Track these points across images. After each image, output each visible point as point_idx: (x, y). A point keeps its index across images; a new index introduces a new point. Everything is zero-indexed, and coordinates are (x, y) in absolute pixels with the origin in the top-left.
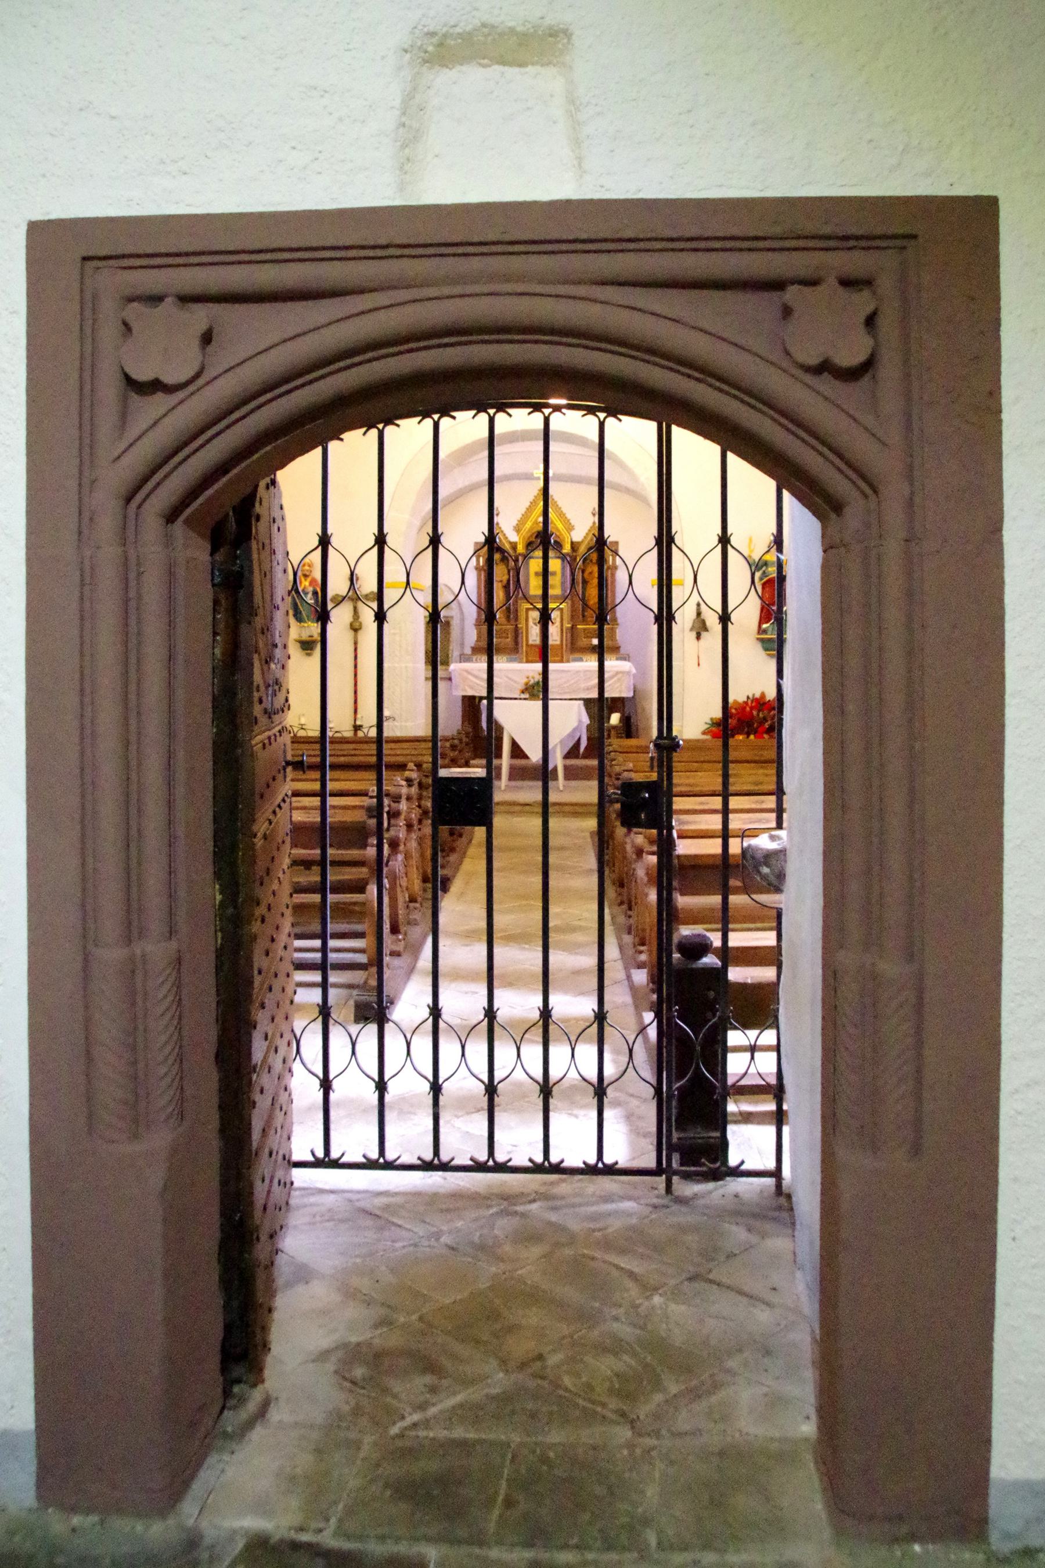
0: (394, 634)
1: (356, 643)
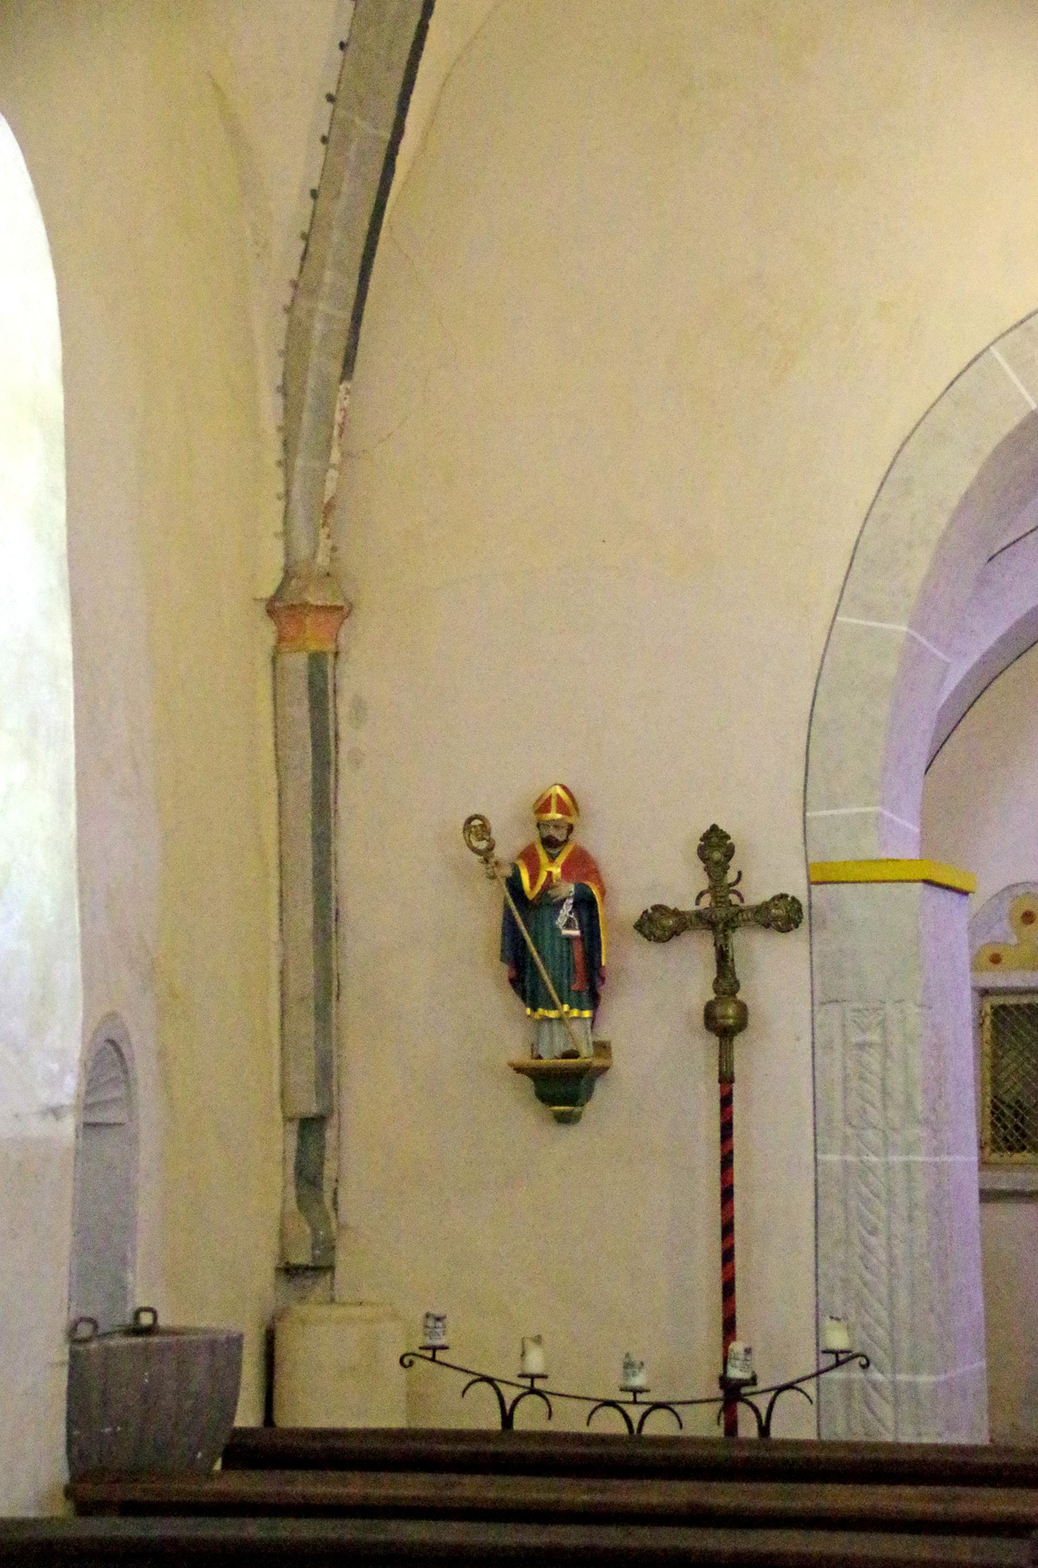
0: (862, 1046)
1: (726, 1080)
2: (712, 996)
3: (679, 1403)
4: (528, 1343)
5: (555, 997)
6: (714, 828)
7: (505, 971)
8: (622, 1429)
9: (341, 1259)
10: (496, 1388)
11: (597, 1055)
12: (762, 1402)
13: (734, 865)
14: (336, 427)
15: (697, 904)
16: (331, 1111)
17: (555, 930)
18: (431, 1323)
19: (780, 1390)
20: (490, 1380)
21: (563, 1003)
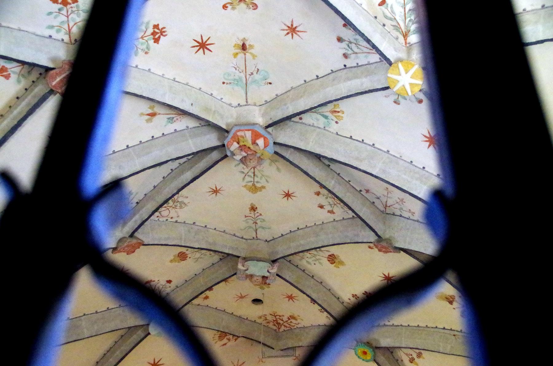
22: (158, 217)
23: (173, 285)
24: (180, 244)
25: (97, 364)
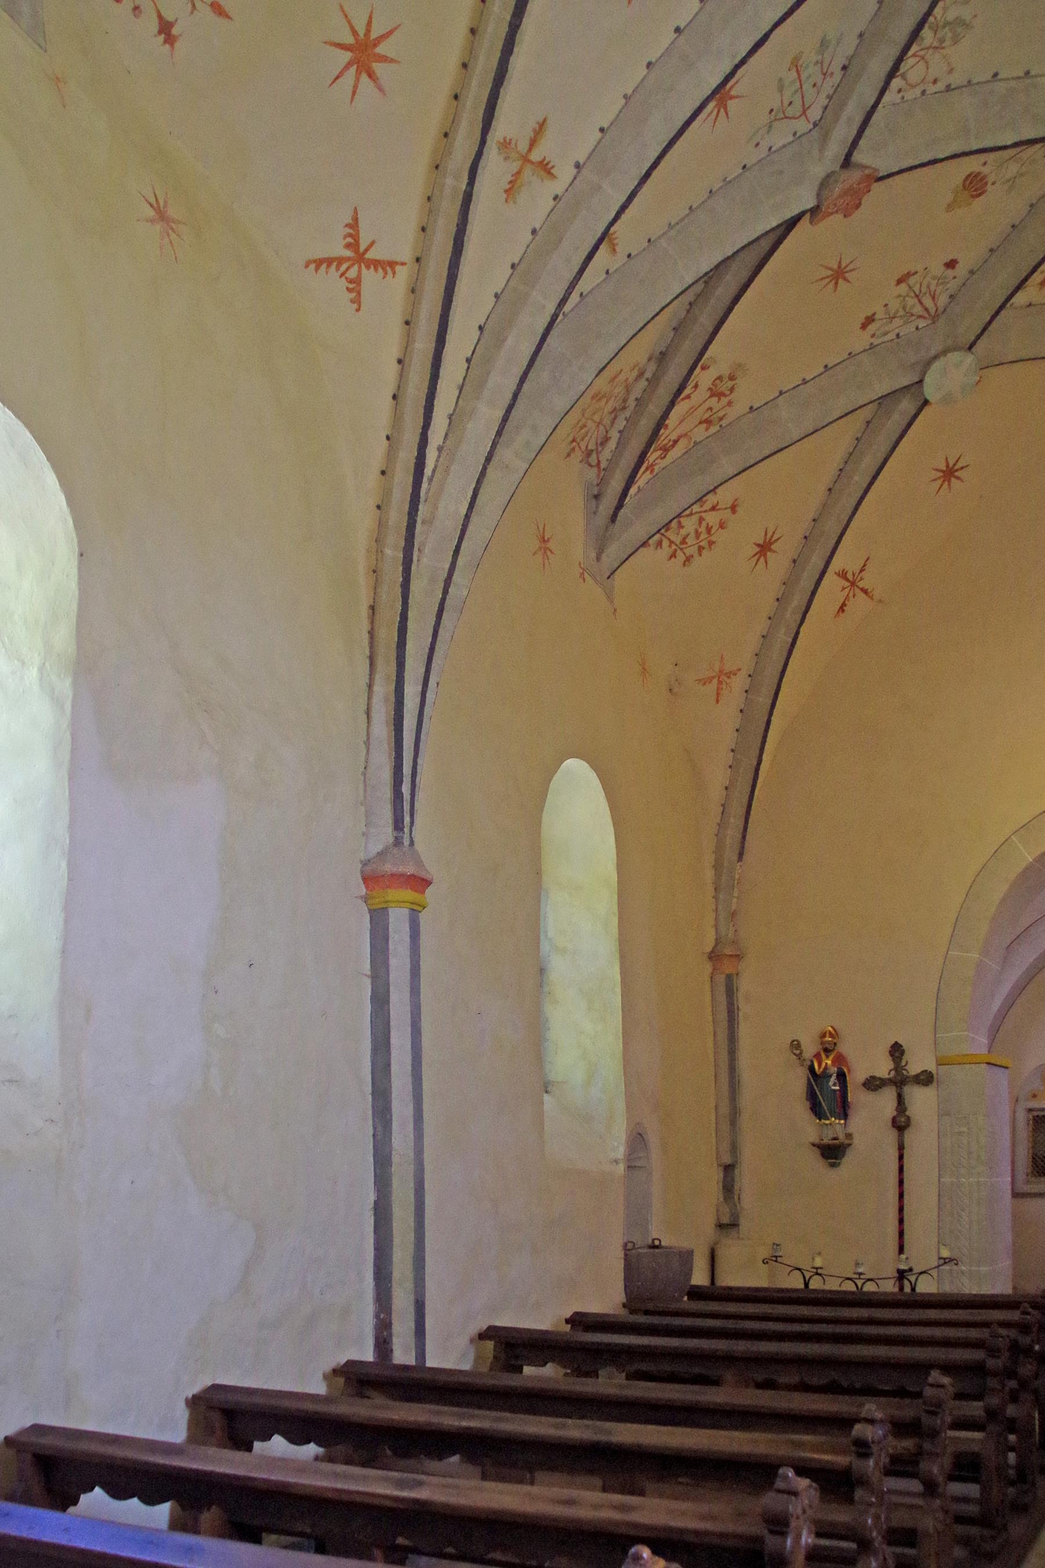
0: (960, 1133)
1: (901, 1148)
2: (895, 1113)
3: (879, 1279)
4: (815, 1255)
5: (829, 1115)
6: (896, 1043)
7: (808, 1104)
8: (854, 1289)
9: (742, 1221)
10: (802, 1273)
11: (846, 1138)
12: (913, 1279)
13: (905, 1058)
14: (736, 881)
15: (889, 1074)
16: (737, 1162)
17: (828, 1087)
18: (775, 1247)
19: (921, 1273)
20: (799, 1269)
21: (832, 1116)
22: (900, 91)
23: (961, 270)
24: (967, 149)
25: (830, 494)
